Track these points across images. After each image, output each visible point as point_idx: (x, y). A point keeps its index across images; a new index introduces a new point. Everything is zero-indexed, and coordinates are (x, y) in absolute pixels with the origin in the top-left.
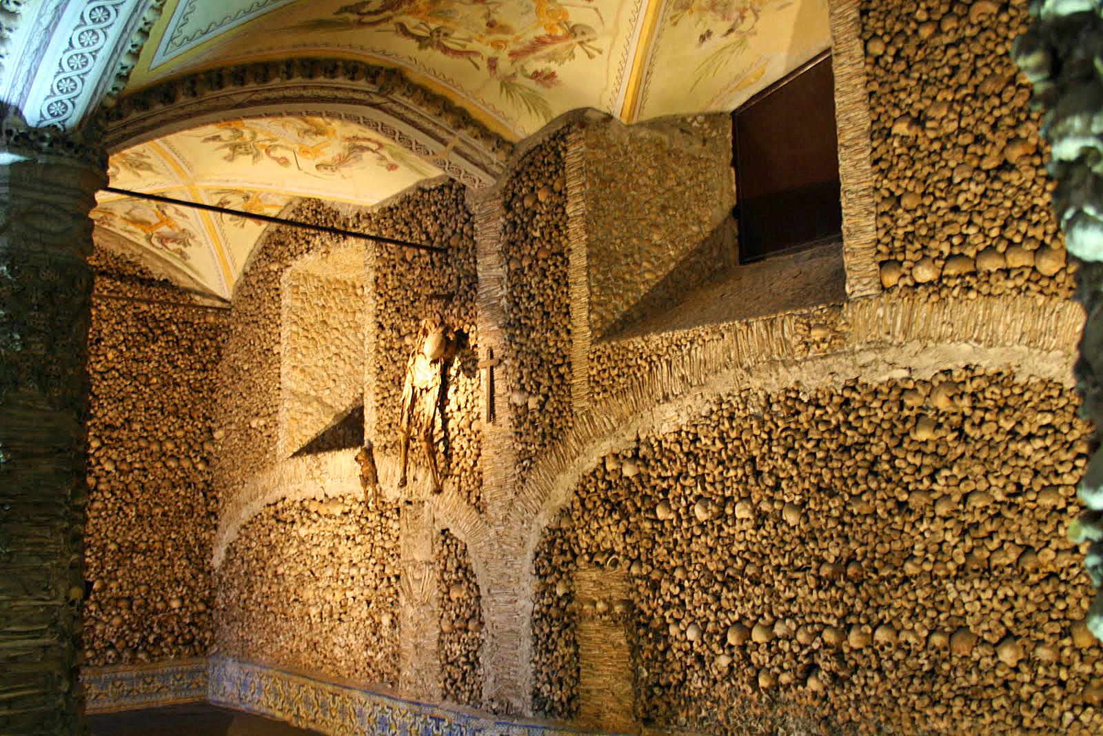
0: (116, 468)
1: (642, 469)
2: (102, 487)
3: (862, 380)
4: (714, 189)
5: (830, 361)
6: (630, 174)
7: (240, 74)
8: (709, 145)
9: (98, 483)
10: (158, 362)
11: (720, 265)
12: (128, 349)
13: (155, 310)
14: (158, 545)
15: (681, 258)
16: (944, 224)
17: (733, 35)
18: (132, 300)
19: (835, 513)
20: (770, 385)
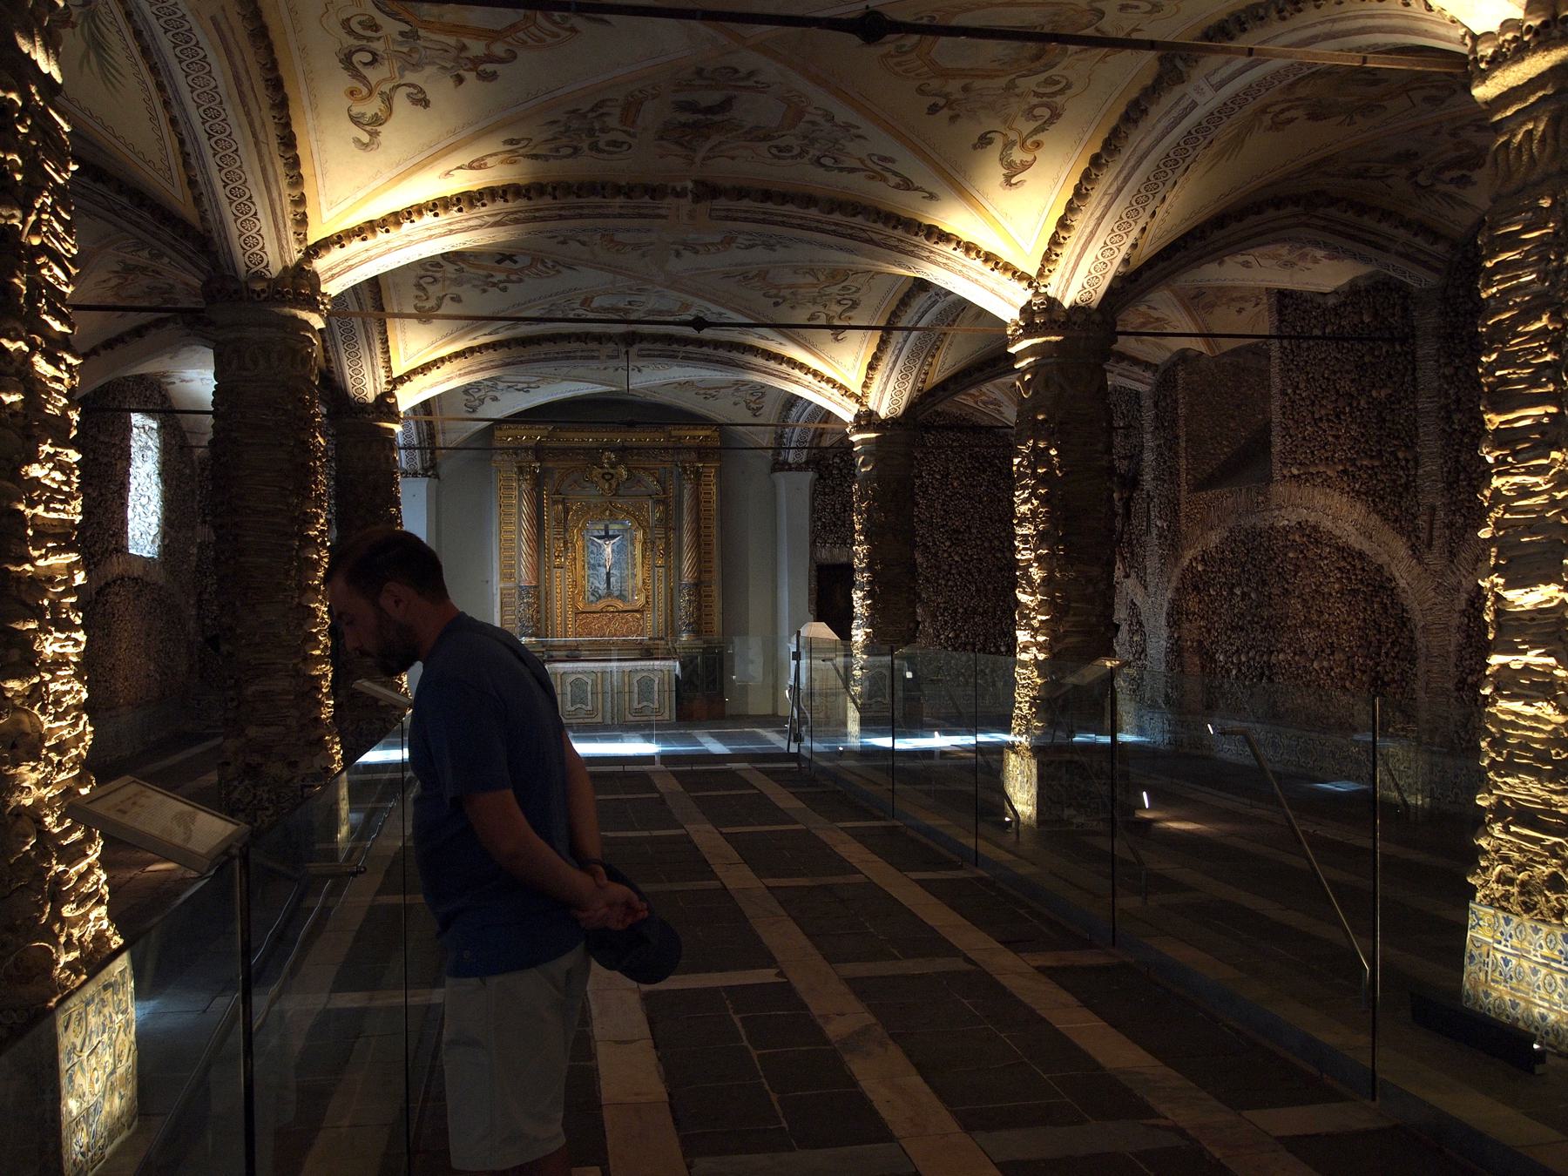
0: (962, 560)
10: (987, 487)
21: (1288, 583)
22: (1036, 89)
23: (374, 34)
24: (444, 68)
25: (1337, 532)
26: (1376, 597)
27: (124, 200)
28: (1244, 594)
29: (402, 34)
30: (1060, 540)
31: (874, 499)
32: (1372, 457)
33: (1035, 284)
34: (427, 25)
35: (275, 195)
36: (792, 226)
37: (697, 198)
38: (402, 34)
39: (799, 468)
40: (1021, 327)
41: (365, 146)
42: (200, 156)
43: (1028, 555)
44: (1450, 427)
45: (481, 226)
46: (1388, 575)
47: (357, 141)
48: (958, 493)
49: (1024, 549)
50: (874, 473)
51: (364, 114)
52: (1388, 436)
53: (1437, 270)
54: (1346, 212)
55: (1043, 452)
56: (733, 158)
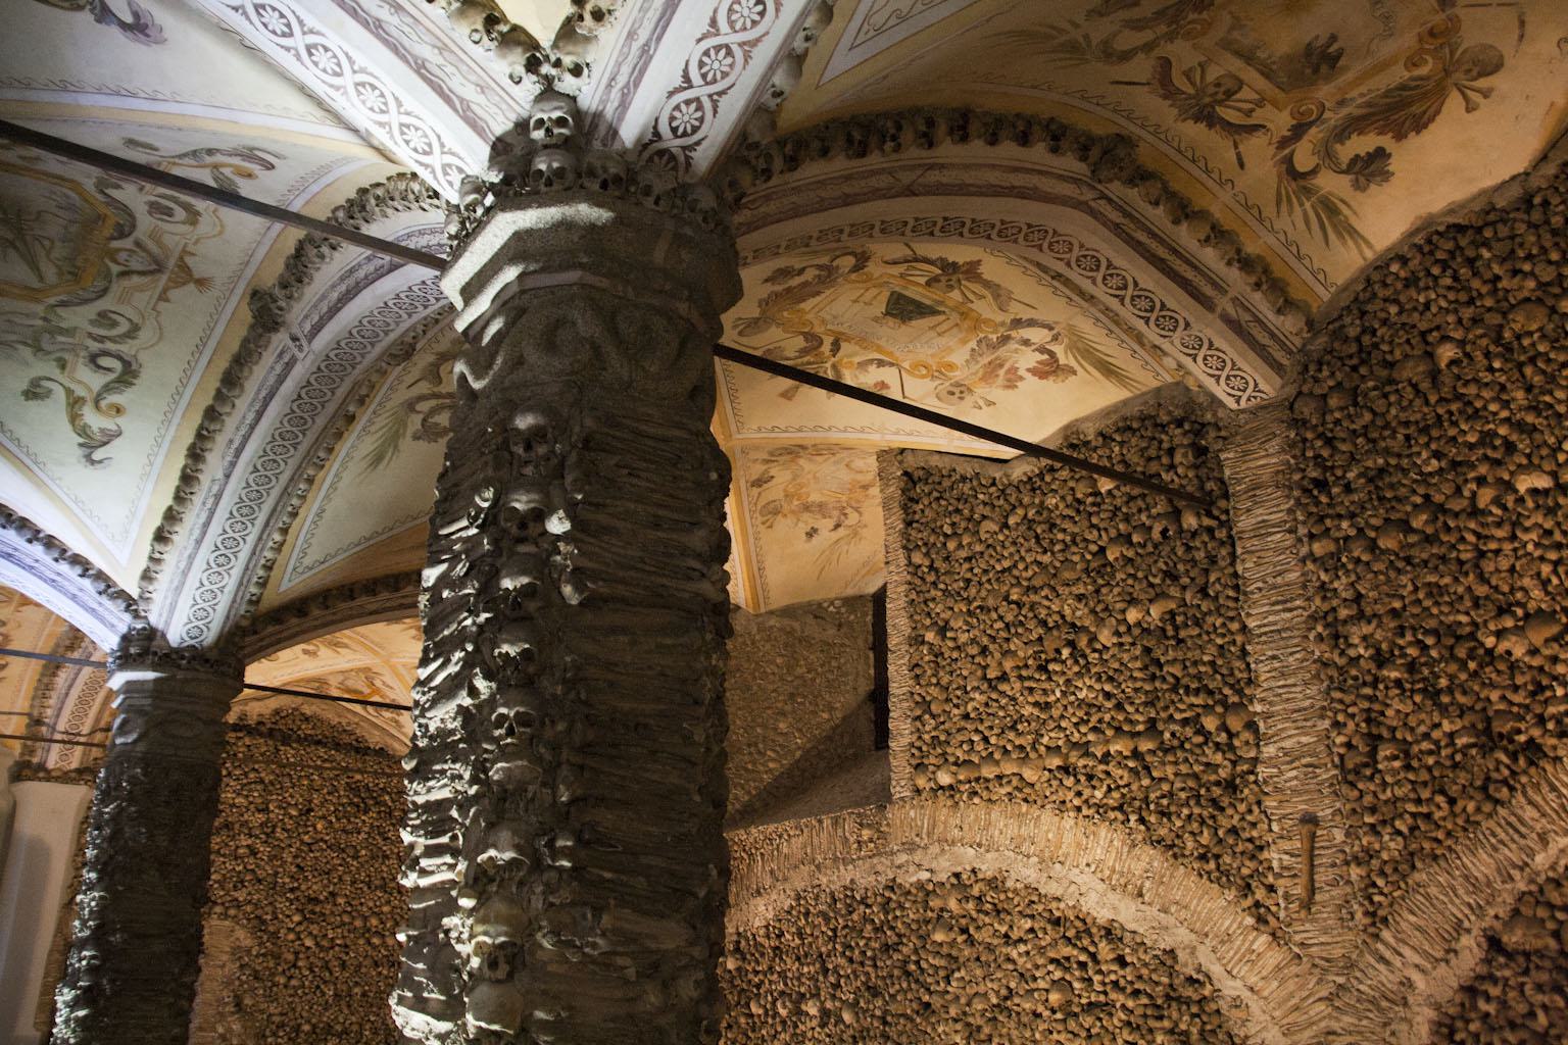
0: (317, 944)
1: (740, 963)
2: (300, 964)
3: (899, 881)
4: (846, 674)
5: (875, 861)
6: (757, 663)
7: (371, 587)
8: (844, 630)
9: (297, 959)
11: (851, 751)
12: (338, 819)
13: (369, 780)
14: (355, 1028)
15: (808, 746)
16: (959, 730)
17: (840, 530)
18: (346, 769)
19: (878, 1013)
20: (833, 882)
21: (931, 993)
25: (1051, 889)
26: (1160, 1018)
28: (825, 1013)
30: (562, 817)
31: (131, 798)
32: (1135, 735)
33: (546, 69)
39: (65, 777)
40: (492, 187)
43: (441, 871)
44: (1342, 653)
46: (1190, 971)
48: (322, 840)
49: (431, 852)
50: (141, 747)
52: (1174, 689)
53: (1278, 368)
54: (1156, 203)
55: (523, 526)
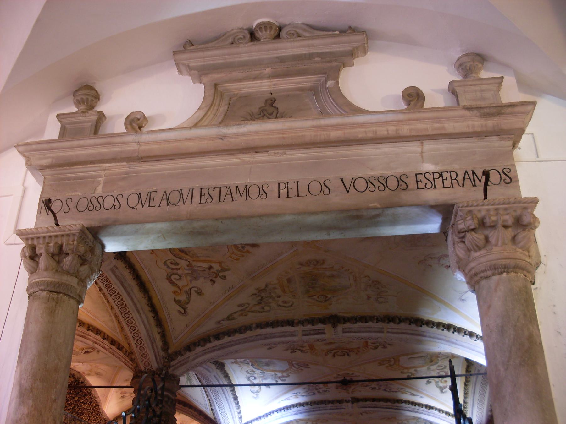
22: (437, 368)
23: (254, 373)
24: (272, 379)
27: (196, 413)
29: (261, 373)
34: (267, 371)
35: (233, 412)
36: (383, 408)
37: (353, 403)
38: (261, 373)
41: (255, 398)
42: (214, 403)
45: (291, 415)
47: (254, 397)
51: (254, 391)
56: (360, 391)
